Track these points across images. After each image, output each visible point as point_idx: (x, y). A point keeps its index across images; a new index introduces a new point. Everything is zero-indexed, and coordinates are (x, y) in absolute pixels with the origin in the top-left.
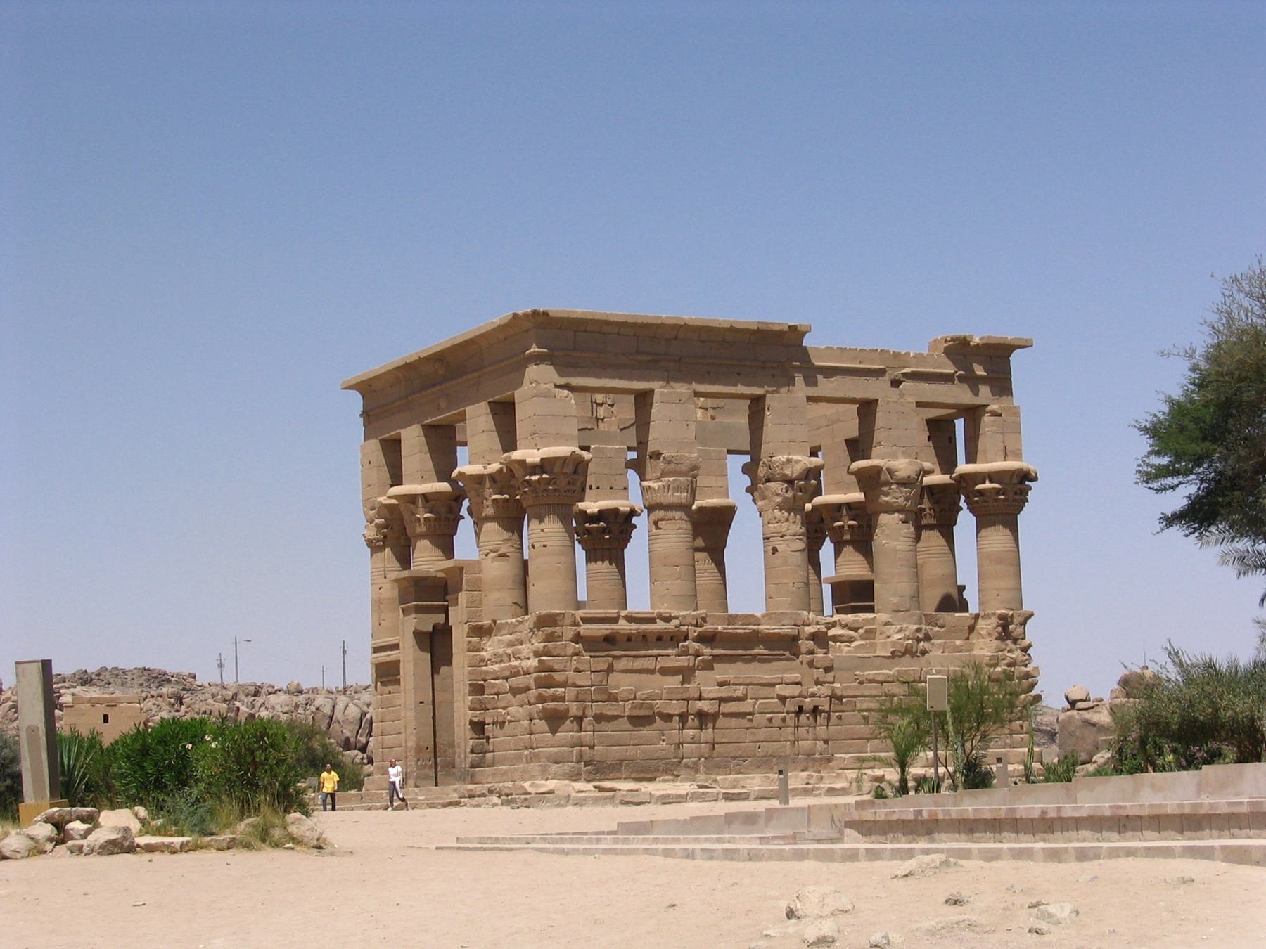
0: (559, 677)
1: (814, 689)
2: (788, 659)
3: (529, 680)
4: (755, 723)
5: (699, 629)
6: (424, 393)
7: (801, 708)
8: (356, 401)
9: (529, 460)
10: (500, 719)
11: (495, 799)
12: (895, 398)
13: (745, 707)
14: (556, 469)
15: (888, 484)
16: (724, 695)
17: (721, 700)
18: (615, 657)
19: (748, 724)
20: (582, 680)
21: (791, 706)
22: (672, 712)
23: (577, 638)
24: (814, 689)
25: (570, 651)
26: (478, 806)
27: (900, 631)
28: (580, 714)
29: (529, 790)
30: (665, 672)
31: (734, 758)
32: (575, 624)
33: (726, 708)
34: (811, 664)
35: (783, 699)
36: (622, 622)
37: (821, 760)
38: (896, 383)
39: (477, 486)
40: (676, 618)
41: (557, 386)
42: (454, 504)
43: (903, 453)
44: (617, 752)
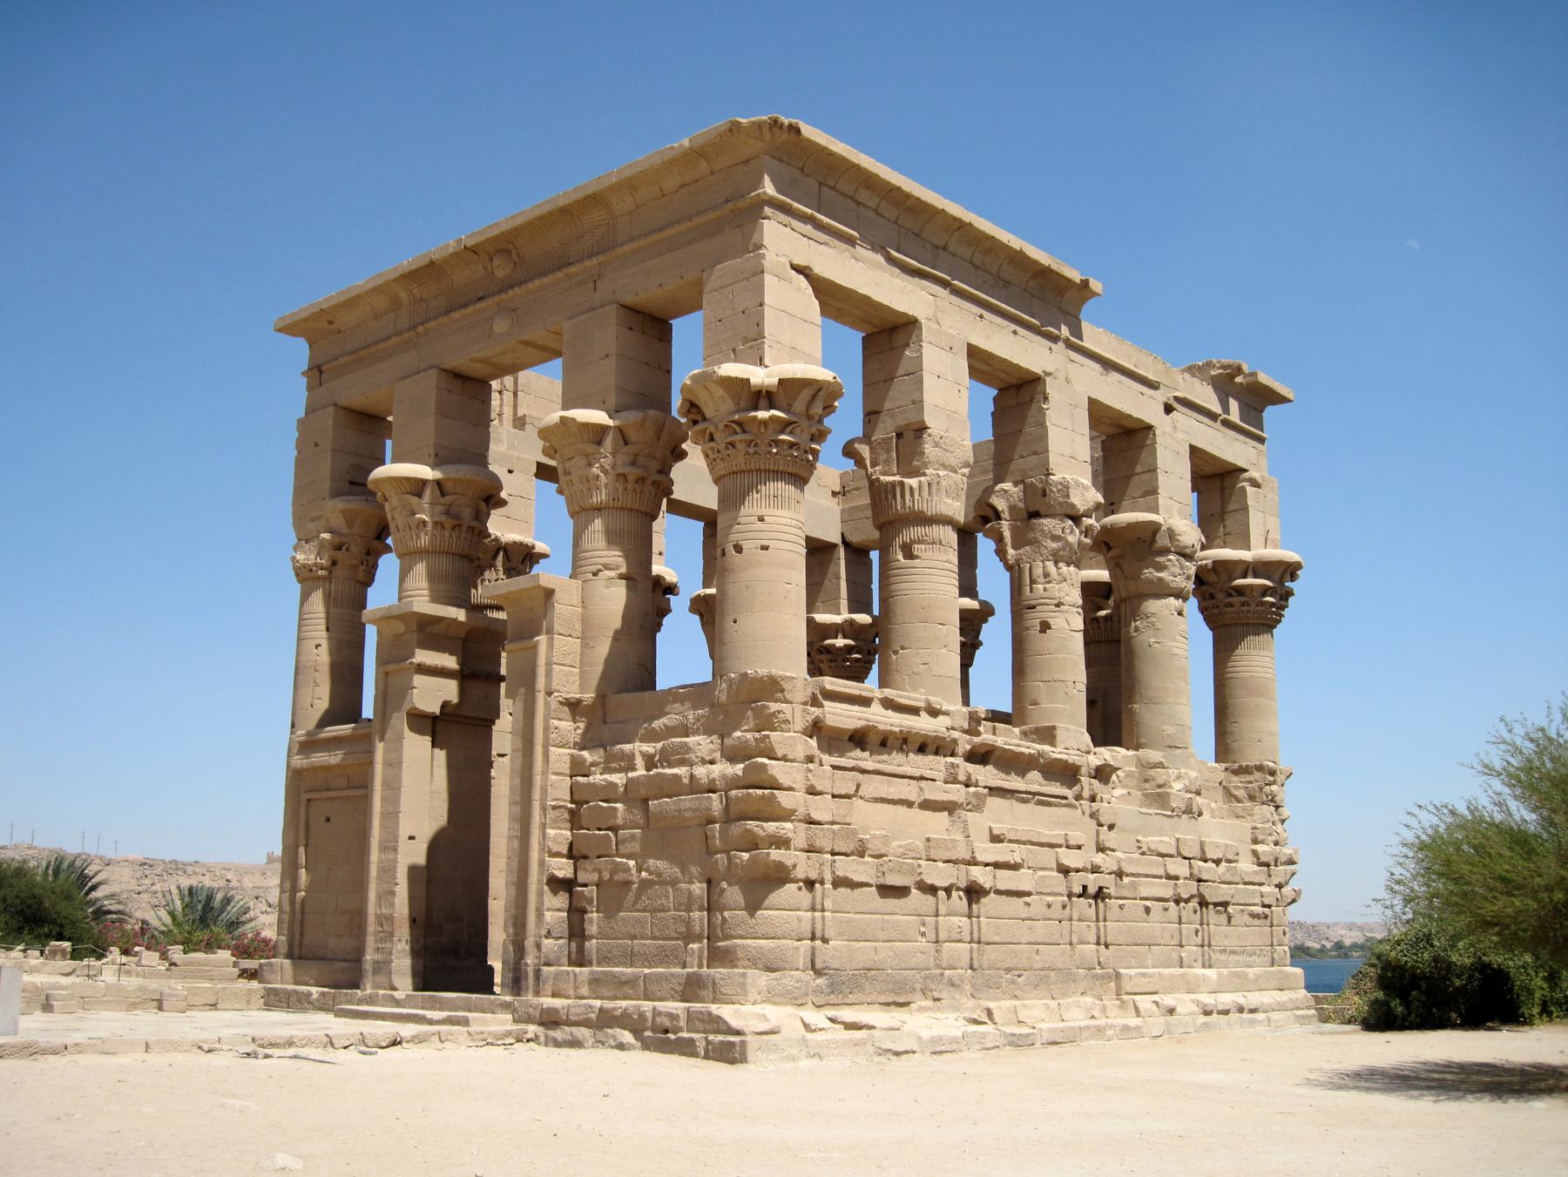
0: (784, 799)
1: (1099, 859)
2: (1070, 806)
3: (716, 802)
4: (1032, 912)
5: (976, 739)
6: (456, 315)
7: (1085, 887)
8: (299, 352)
9: (753, 381)
10: (620, 877)
11: (627, 1037)
12: (1169, 430)
13: (1021, 880)
14: (799, 405)
15: (1166, 551)
16: (1001, 858)
17: (997, 865)
18: (863, 771)
19: (1024, 913)
20: (822, 809)
21: (1078, 889)
22: (938, 883)
23: (816, 729)
24: (1099, 859)
25: (800, 753)
26: (575, 1043)
27: (1178, 778)
28: (813, 875)
29: (734, 1023)
30: (928, 805)
31: (1008, 970)
32: (814, 702)
33: (1006, 880)
34: (1093, 815)
35: (1065, 871)
36: (876, 707)
37: (1103, 977)
38: (1168, 409)
39: (590, 448)
40: (946, 713)
41: (794, 267)
42: (483, 505)
43: (1179, 511)
44: (864, 953)
